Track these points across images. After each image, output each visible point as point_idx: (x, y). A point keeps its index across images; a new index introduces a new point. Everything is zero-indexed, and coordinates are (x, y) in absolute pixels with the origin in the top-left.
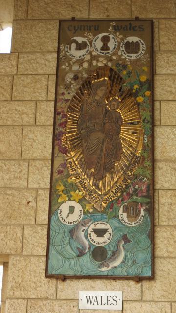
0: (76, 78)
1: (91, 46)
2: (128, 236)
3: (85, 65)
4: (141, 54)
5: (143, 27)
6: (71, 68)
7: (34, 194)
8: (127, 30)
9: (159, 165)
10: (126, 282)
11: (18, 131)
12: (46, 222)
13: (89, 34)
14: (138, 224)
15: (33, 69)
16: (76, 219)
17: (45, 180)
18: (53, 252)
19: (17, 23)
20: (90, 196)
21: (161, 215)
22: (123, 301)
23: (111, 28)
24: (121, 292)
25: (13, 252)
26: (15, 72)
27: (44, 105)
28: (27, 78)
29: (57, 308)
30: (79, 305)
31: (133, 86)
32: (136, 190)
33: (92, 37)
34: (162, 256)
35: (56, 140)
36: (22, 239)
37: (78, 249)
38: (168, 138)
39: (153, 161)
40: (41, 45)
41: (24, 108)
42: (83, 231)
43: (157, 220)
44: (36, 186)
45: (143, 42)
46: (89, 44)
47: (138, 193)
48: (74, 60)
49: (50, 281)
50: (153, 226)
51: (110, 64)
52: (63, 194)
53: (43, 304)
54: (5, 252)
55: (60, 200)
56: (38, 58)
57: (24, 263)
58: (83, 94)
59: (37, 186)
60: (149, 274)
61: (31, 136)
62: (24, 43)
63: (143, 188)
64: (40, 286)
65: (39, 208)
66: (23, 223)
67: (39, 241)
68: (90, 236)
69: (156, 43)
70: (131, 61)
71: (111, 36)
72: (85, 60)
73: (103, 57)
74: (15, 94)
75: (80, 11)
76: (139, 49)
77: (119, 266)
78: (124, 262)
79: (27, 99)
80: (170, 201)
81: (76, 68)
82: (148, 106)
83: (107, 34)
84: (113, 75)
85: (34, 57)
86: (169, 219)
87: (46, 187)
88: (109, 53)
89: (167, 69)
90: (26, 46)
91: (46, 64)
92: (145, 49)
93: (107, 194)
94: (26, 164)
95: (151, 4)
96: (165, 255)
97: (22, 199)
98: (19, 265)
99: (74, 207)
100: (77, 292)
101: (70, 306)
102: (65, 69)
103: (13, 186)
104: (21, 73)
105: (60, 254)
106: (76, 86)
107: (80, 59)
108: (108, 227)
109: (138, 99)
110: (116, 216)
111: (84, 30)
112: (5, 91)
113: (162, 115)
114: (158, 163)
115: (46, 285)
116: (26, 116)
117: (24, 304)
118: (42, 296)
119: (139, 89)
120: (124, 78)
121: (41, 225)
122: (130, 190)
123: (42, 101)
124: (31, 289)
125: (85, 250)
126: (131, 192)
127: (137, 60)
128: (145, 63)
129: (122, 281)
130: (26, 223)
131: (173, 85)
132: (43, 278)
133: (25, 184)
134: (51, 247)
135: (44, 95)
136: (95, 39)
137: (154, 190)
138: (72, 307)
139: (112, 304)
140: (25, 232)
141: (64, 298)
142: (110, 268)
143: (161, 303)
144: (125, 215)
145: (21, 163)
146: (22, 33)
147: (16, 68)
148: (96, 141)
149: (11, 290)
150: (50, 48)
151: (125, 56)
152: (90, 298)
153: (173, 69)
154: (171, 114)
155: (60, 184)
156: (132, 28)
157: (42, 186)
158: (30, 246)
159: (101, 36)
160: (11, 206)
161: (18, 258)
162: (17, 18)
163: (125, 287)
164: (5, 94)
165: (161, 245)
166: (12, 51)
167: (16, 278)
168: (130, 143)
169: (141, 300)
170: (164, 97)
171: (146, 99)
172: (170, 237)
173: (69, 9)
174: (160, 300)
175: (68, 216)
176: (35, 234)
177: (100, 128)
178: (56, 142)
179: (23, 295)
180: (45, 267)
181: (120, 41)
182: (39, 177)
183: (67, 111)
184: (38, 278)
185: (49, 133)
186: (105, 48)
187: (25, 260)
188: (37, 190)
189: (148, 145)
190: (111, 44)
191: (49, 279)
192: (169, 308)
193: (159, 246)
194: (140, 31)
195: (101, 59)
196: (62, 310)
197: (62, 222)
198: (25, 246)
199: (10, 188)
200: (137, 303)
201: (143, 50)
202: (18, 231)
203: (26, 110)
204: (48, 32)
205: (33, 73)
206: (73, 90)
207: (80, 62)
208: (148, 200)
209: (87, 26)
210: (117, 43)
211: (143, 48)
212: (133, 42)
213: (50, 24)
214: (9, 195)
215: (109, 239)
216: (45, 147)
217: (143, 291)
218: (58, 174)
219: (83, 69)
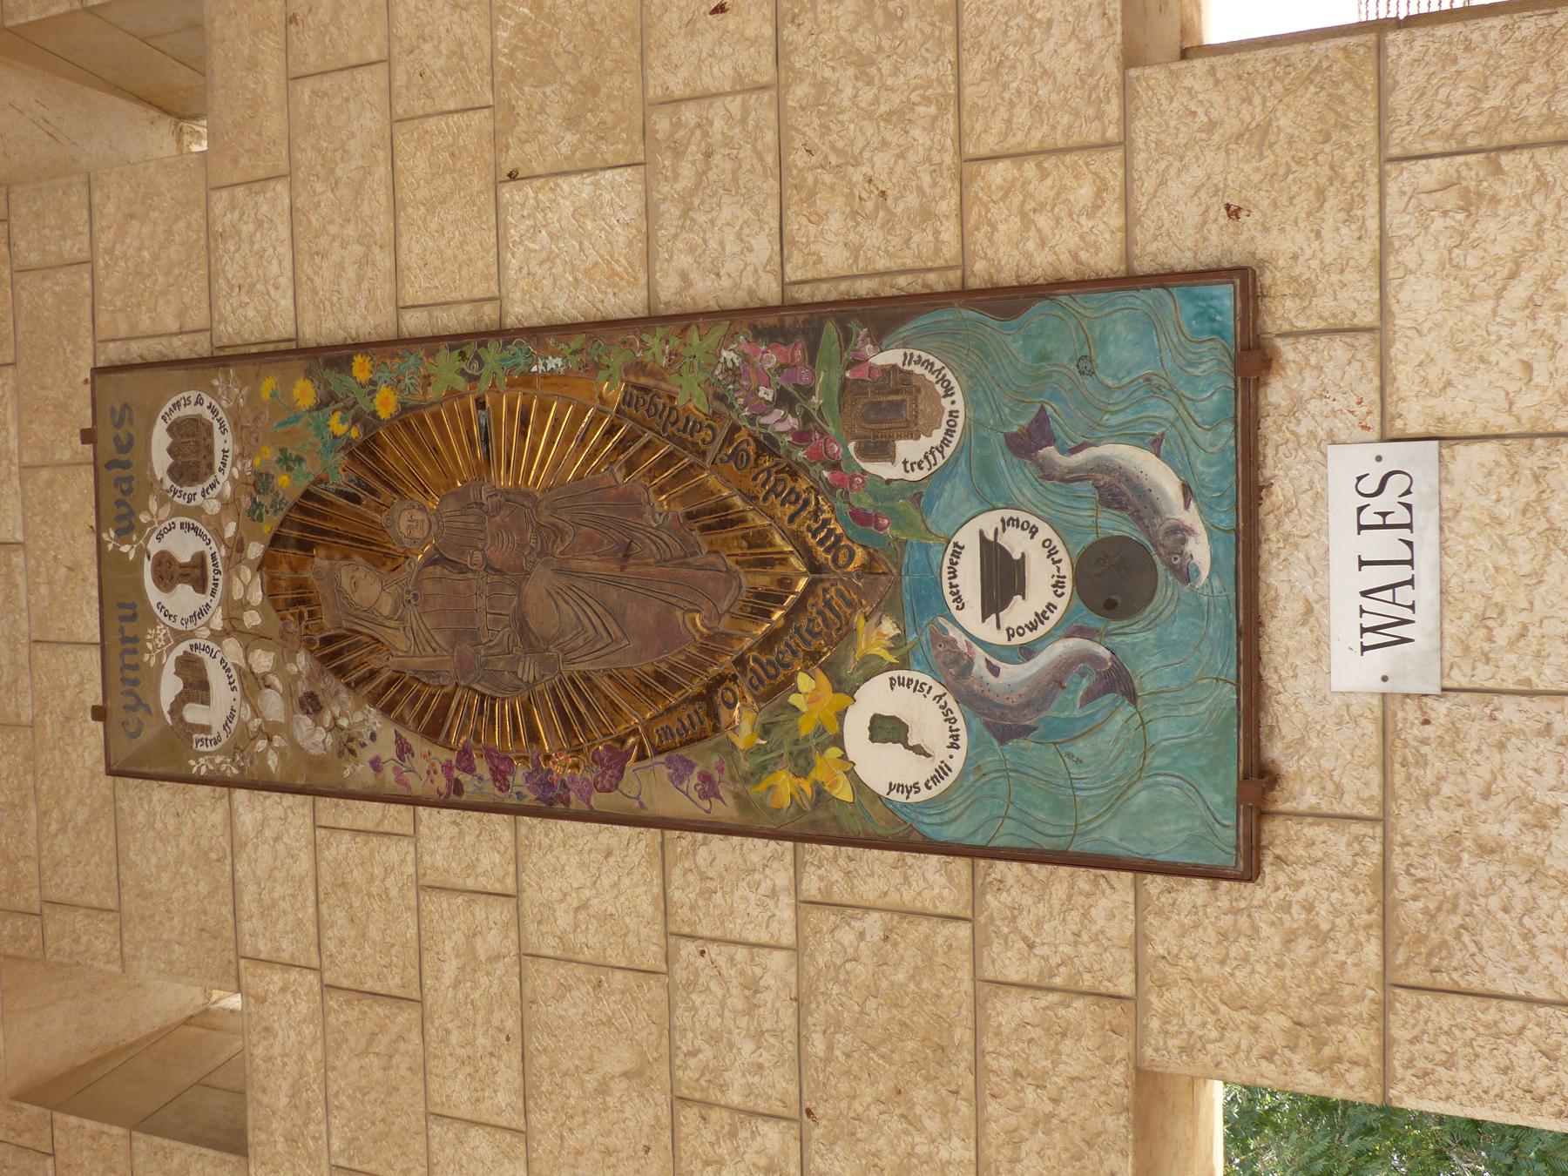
0: (311, 704)
1: (191, 635)
2: (1015, 429)
3: (263, 661)
4: (214, 412)
5: (118, 408)
6: (277, 727)
7: (824, 919)
8: (130, 479)
9: (669, 292)
10: (1268, 425)
11: (545, 978)
12: (961, 865)
13: (150, 646)
14: (950, 376)
15: (294, 896)
16: (935, 707)
17: (755, 858)
18: (1111, 837)
19: (134, 957)
20: (815, 635)
21: (909, 262)
22: (1384, 439)
23: (125, 548)
24: (1332, 450)
25: (1122, 1048)
26: (312, 977)
27: (433, 853)
28: (332, 925)
29: (1437, 821)
30: (1416, 687)
31: (335, 437)
32: (784, 399)
33: (161, 631)
34: (1120, 235)
35: (567, 802)
36: (1053, 998)
37: (1090, 697)
38: (550, 259)
39: (650, 321)
40: (206, 854)
41: (448, 946)
42: (995, 671)
43: (932, 277)
44: (785, 910)
45: (169, 405)
46: (184, 647)
47: (797, 386)
48: (246, 713)
49: (1278, 851)
50: (965, 295)
51: (255, 550)
52: (813, 775)
53: (1415, 898)
54: (1126, 1095)
55: (844, 792)
56: (254, 873)
57: (1180, 993)
58: (373, 674)
59: (786, 900)
60: (1224, 297)
61: (563, 920)
62: (203, 930)
63: (772, 359)
64: (1309, 908)
65: (893, 898)
66: (967, 985)
67: (1056, 902)
68: (1020, 631)
69: (180, 348)
70: (242, 455)
71: (154, 547)
72: (242, 664)
73: (228, 581)
74: (393, 984)
75: (82, 683)
76: (196, 421)
77: (1183, 470)
78: (1155, 445)
79: (412, 932)
80: (835, 222)
81: (274, 705)
82: (413, 361)
83: (148, 566)
84: (295, 534)
85: (252, 888)
86: (926, 214)
87: (789, 858)
88: (213, 556)
89: (277, 288)
90: (212, 923)
91: (276, 839)
92: (193, 395)
93: (804, 543)
94: (688, 949)
95: (49, 381)
96: (1117, 221)
97: (847, 981)
98: (1193, 1022)
99: (876, 719)
100: (1337, 701)
101: (1425, 741)
102: (281, 753)
103: (788, 1019)
104: (313, 949)
105: (1116, 800)
106: (341, 704)
107: (243, 688)
108: (968, 538)
109: (384, 414)
110: (917, 494)
111: (136, 667)
112: (383, 1029)
113: (456, 296)
114: (663, 299)
115: (1304, 875)
116: (479, 939)
117: (1419, 1006)
118: (1368, 898)
119: (346, 409)
120: (303, 484)
121: (976, 892)
122: (781, 427)
123: (417, 861)
124: (1330, 965)
125: (1094, 659)
126: (793, 422)
127: (236, 424)
128: (245, 391)
129: (1270, 451)
130: (968, 966)
131: (335, 257)
132: (1260, 894)
133: (778, 960)
134: (1084, 845)
135: (393, 852)
136: (166, 620)
137: (788, 306)
138: (1428, 731)
139: (1406, 499)
140: (1015, 978)
141: (1375, 776)
142: (1191, 517)
143: (1395, 221)
144: (908, 449)
145: (680, 975)
146: (165, 937)
147: (294, 974)
148: (563, 606)
149: (1339, 1077)
150: (218, 817)
151: (224, 482)
152: (1374, 630)
153: (275, 262)
154: (449, 253)
155: (762, 787)
156: (123, 457)
157: (783, 878)
158: (1088, 951)
159: (153, 594)
160: (884, 1042)
161: (1155, 1024)
162: (116, 954)
163: (1302, 430)
164: (395, 1029)
165: (1061, 249)
166: (234, 986)
167: (1264, 1042)
168: (567, 438)
169: (1380, 333)
170: (384, 291)
171: (386, 375)
172: (1016, 199)
173: (77, 731)
174: (1373, 225)
175: (919, 750)
176: (1024, 924)
177: (509, 591)
178: (576, 803)
179: (1364, 1008)
180: (1200, 884)
181: (167, 509)
182: (743, 889)
183: (446, 745)
184: (1262, 918)
185: (547, 835)
186: (195, 573)
187: (1163, 985)
188: (803, 904)
189: (575, 352)
190: (184, 547)
191: (1268, 858)
192: (1419, 166)
193: (1065, 257)
194: (131, 421)
195: (238, 594)
196: (1447, 789)
197: (952, 777)
198: (1087, 982)
199: (800, 1039)
200: (1396, 350)
201: (199, 402)
202: (1011, 1011)
203: (458, 937)
204: (159, 825)
205: (312, 898)
206: (359, 717)
207: (250, 684)
208: (831, 331)
209: (123, 654)
210: (178, 520)
211: (192, 404)
212: (170, 451)
213: (133, 815)
214: (830, 1048)
215: (1034, 531)
216: (609, 854)
217: (1322, 325)
218: (717, 796)
219: (278, 668)
